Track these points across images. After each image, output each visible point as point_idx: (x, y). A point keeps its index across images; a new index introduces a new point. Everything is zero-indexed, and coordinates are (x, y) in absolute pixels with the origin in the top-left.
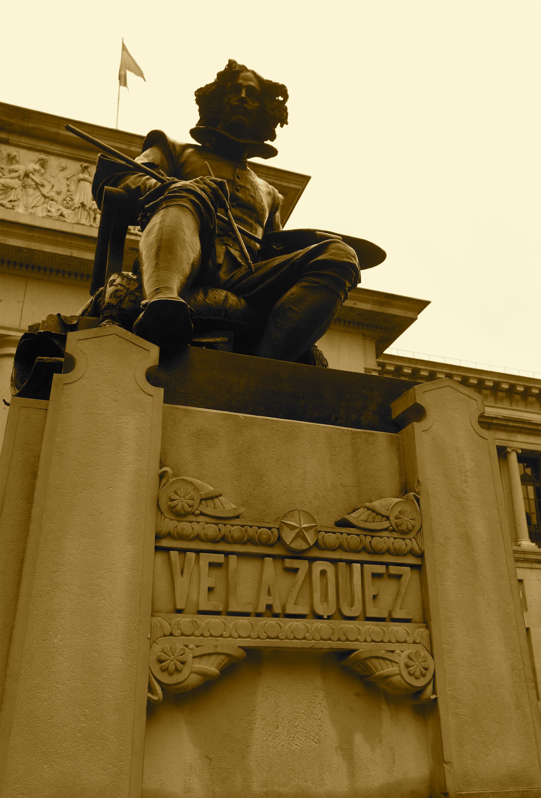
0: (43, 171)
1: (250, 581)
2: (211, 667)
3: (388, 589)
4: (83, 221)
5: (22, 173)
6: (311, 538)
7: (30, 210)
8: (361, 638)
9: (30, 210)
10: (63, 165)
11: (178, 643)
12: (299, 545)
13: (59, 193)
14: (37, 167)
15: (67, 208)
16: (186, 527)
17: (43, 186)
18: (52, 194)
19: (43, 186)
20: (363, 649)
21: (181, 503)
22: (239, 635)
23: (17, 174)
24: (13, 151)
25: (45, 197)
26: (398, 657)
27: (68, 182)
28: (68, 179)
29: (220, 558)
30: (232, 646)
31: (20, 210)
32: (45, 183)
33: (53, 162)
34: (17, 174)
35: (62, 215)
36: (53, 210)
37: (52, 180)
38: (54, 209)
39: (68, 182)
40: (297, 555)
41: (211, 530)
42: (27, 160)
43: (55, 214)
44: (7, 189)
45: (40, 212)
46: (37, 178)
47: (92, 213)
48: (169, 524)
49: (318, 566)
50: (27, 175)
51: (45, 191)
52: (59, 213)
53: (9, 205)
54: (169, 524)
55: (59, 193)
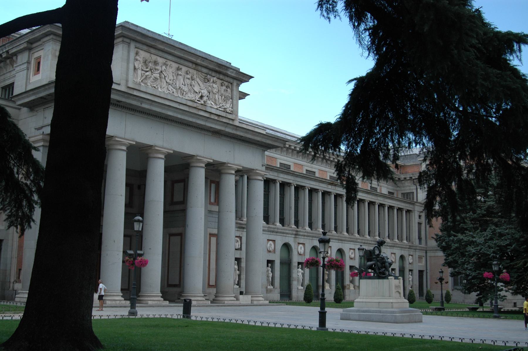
4: (180, 96)
13: (170, 80)
24: (154, 57)
50: (161, 72)
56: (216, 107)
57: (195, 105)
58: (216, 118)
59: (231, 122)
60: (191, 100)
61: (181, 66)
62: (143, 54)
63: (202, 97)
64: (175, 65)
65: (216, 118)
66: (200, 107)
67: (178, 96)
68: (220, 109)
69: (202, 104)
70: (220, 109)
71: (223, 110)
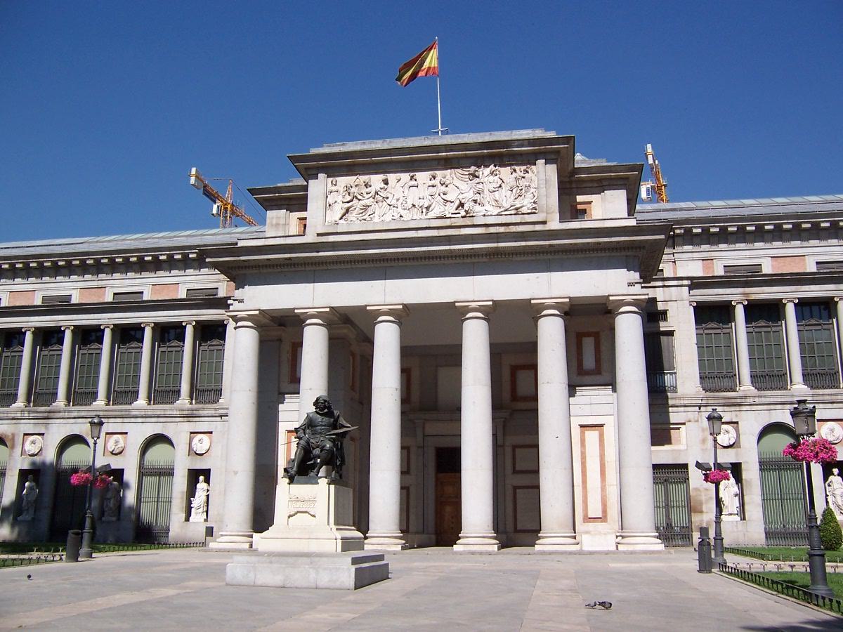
0: (386, 186)
2: (294, 513)
3: (313, 504)
5: (373, 193)
7: (382, 218)
9: (382, 218)
10: (398, 178)
14: (383, 185)
15: (404, 209)
17: (387, 198)
18: (394, 202)
19: (387, 198)
20: (308, 511)
23: (370, 195)
25: (390, 205)
27: (403, 190)
28: (402, 187)
30: (296, 511)
31: (376, 219)
32: (389, 195)
33: (392, 177)
34: (370, 195)
35: (401, 216)
36: (395, 214)
37: (392, 191)
38: (395, 213)
39: (403, 190)
42: (376, 180)
43: (397, 217)
44: (366, 207)
45: (388, 218)
46: (383, 194)
47: (420, 209)
51: (388, 201)
52: (399, 215)
53: (368, 219)
55: (398, 200)
56: (497, 213)
57: (447, 222)
58: (502, 229)
59: (538, 228)
60: (438, 218)
61: (412, 174)
62: (343, 181)
63: (462, 205)
64: (405, 177)
65: (502, 229)
66: (461, 222)
67: (414, 218)
68: (506, 213)
69: (462, 217)
70: (506, 213)
71: (513, 212)
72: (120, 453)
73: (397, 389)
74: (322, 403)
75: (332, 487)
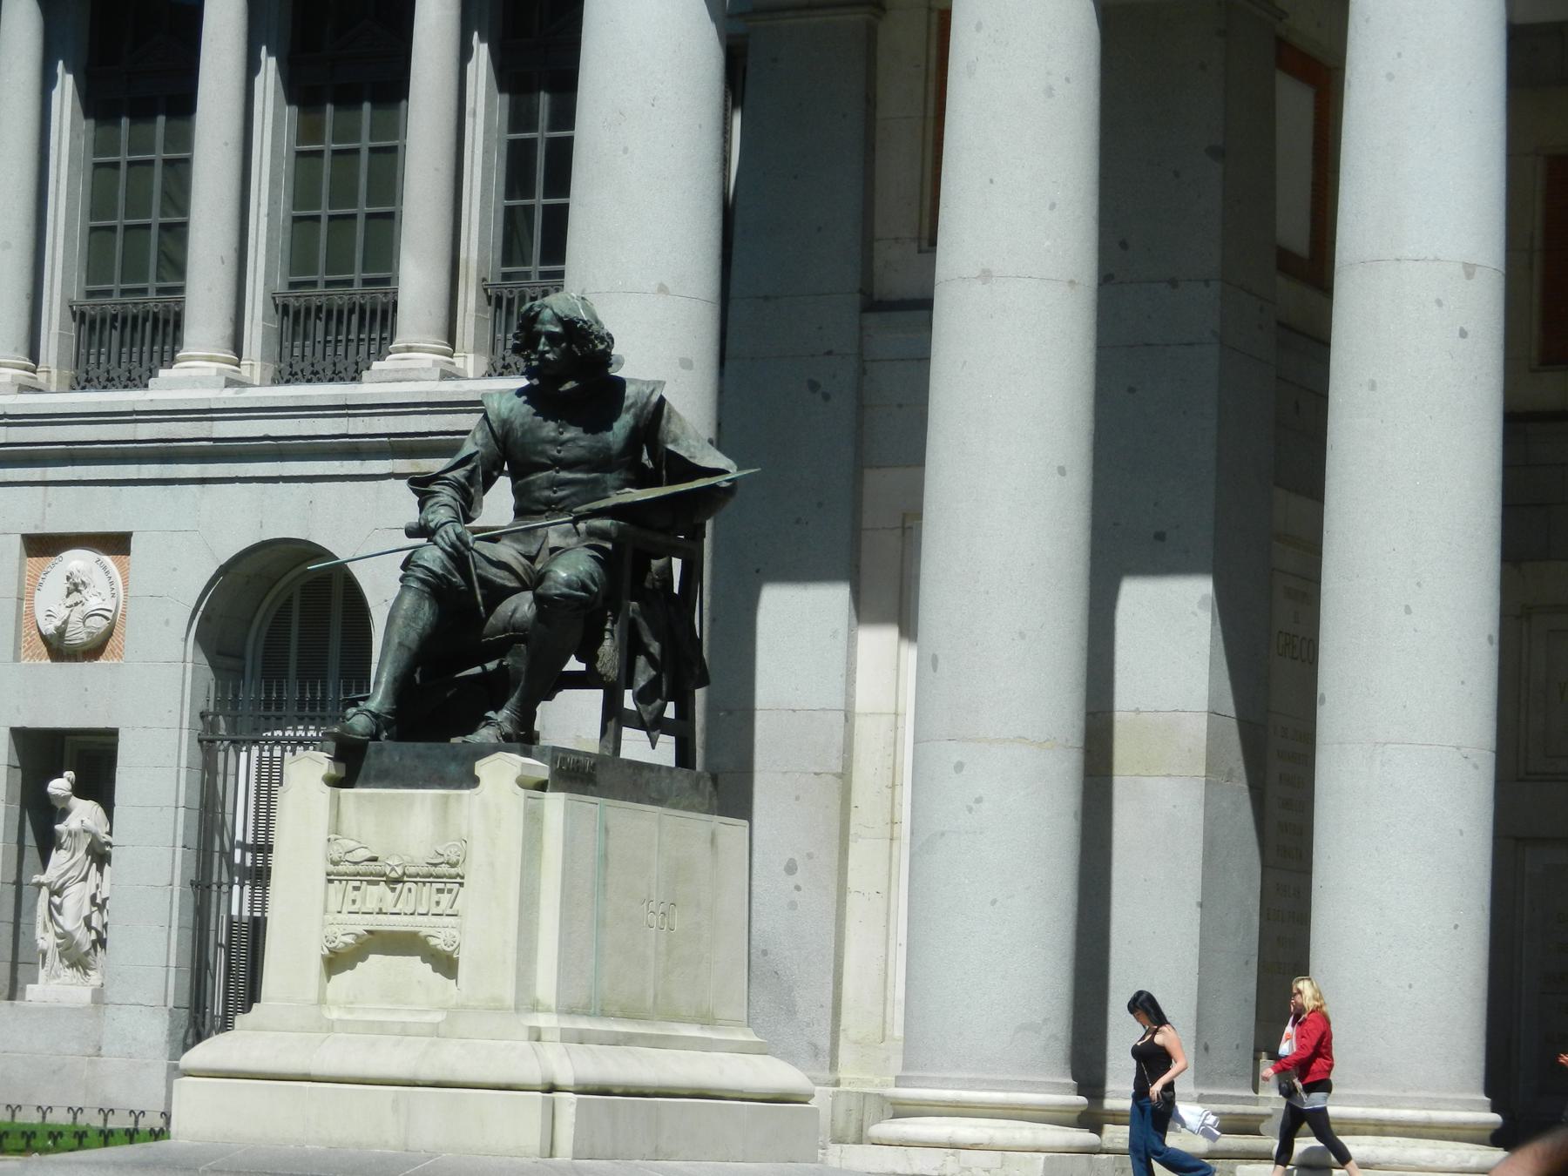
1: (377, 894)
3: (445, 898)
6: (400, 871)
8: (422, 925)
11: (335, 928)
12: (393, 875)
16: (342, 868)
20: (424, 932)
21: (336, 857)
22: (361, 924)
26: (441, 936)
29: (357, 884)
40: (397, 881)
41: (352, 868)
48: (331, 868)
49: (407, 885)
54: (331, 868)
72: (94, 650)
73: (1469, 270)
74: (551, 337)
75: (555, 803)
